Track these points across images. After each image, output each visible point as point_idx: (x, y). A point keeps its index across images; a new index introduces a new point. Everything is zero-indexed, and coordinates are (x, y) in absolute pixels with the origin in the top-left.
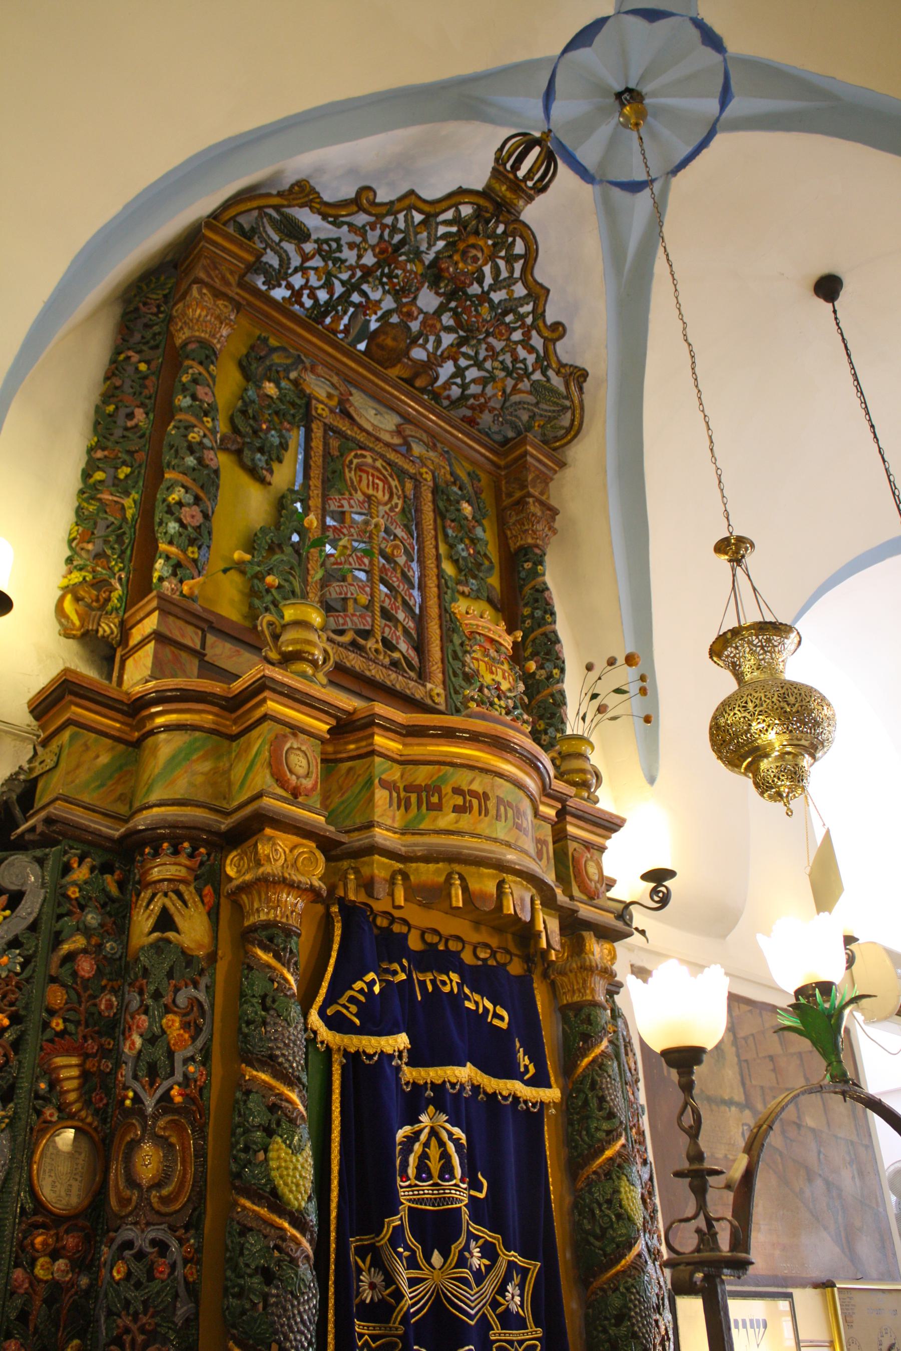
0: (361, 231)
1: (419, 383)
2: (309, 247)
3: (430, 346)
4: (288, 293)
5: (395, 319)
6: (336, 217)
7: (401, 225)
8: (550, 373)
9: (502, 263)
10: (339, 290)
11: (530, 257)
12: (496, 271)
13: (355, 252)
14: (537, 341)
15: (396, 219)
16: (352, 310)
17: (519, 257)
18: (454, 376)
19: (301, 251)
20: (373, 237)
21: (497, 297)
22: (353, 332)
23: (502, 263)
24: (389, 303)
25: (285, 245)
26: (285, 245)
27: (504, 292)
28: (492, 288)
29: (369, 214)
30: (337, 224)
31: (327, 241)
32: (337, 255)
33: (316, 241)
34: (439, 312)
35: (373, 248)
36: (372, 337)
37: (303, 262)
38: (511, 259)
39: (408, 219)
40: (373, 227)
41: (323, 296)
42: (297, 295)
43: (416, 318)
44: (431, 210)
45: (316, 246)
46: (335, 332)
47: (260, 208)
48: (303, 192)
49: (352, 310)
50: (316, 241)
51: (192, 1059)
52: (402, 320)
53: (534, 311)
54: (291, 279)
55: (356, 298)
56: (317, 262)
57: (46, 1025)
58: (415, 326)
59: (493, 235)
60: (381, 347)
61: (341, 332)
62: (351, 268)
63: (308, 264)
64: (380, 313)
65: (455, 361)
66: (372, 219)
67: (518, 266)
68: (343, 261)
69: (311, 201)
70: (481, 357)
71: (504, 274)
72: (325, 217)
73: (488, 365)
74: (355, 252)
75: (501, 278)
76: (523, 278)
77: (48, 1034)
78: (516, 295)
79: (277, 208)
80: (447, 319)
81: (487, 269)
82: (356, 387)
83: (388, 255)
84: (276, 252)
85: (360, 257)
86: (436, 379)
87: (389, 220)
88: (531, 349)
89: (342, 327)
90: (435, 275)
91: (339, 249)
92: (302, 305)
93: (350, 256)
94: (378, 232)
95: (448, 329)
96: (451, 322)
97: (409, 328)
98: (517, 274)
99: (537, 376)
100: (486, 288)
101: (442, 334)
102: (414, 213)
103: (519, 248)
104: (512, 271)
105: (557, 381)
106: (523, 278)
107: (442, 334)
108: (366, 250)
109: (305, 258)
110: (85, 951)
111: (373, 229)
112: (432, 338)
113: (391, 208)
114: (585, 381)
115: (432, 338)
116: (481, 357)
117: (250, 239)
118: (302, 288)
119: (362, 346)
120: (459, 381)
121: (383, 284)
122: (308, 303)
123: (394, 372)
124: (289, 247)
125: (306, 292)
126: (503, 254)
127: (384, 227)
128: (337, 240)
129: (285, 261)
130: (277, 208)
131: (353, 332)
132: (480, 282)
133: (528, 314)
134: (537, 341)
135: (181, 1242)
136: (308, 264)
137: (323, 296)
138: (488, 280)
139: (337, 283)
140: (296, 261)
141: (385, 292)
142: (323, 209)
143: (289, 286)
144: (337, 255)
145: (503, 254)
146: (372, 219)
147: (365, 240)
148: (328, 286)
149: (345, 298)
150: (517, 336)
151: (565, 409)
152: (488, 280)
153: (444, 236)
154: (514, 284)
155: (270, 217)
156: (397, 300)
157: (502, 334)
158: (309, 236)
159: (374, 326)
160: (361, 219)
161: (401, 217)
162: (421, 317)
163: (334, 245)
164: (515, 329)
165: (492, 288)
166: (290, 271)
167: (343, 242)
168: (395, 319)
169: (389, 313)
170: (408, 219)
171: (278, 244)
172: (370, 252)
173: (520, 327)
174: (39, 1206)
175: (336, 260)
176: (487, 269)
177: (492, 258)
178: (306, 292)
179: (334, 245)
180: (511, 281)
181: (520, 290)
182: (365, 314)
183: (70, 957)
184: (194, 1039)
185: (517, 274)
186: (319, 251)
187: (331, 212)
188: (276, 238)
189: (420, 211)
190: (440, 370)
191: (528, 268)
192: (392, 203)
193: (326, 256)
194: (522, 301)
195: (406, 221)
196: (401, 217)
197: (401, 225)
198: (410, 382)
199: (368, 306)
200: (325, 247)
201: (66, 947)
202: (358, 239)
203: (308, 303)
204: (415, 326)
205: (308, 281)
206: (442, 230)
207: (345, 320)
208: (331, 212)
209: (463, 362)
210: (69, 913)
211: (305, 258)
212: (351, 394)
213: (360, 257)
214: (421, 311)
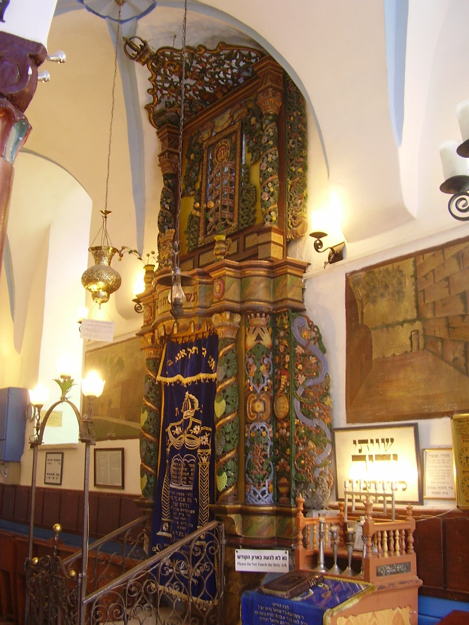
0: (163, 95)
7: (161, 84)
8: (221, 53)
14: (207, 55)
15: (159, 86)
31: (166, 105)
39: (160, 81)
62: (177, 100)
66: (159, 91)
68: (174, 102)
73: (218, 70)
85: (173, 96)
87: (160, 88)
88: (210, 57)
97: (201, 90)
99: (223, 57)
105: (226, 52)
114: (225, 43)
120: (225, 81)
128: (166, 102)
130: (153, 115)
134: (207, 55)
142: (155, 104)
146: (159, 91)
147: (167, 94)
150: (205, 60)
151: (239, 51)
158: (164, 110)
160: (159, 95)
161: (158, 84)
164: (201, 60)
167: (167, 100)
191: (177, 51)
196: (158, 84)
197: (161, 84)
202: (166, 97)
206: (162, 72)
213: (173, 96)
214: (194, 85)
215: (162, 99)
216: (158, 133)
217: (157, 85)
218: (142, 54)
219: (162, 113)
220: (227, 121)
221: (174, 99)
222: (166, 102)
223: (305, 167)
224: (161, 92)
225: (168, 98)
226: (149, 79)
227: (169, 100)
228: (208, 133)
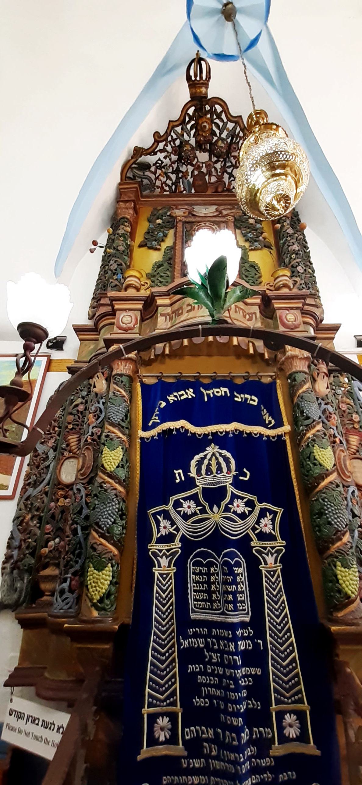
1: (220, 190)
2: (153, 169)
3: (214, 173)
4: (159, 190)
5: (196, 173)
6: (153, 151)
7: (175, 137)
9: (217, 121)
10: (173, 177)
11: (225, 109)
12: (217, 125)
13: (168, 159)
15: (172, 136)
16: (181, 180)
17: (221, 112)
18: (229, 178)
19: (152, 172)
20: (169, 148)
21: (224, 136)
22: (187, 188)
23: (217, 121)
24: (190, 168)
25: (146, 173)
26: (146, 173)
27: (225, 131)
28: (220, 134)
29: (162, 141)
30: (155, 154)
31: (156, 162)
32: (163, 165)
33: (153, 165)
34: (210, 159)
35: (172, 153)
36: (194, 185)
37: (155, 175)
38: (219, 116)
39: (176, 133)
40: (166, 145)
41: (169, 182)
42: (162, 188)
43: (202, 166)
44: (182, 122)
45: (154, 167)
46: (182, 192)
47: (130, 167)
48: (138, 152)
49: (181, 180)
50: (153, 165)
51: (95, 427)
52: (199, 172)
53: (241, 130)
54: (157, 184)
55: (180, 175)
56: (159, 172)
57: (67, 427)
58: (204, 170)
59: (207, 112)
60: (200, 186)
61: (184, 191)
62: (170, 166)
63: (157, 176)
64: (190, 174)
65: (226, 171)
66: (164, 143)
67: (223, 116)
69: (142, 152)
70: (234, 163)
71: (221, 124)
72: (150, 154)
74: (168, 159)
75: (221, 126)
76: (229, 120)
77: (67, 430)
78: (230, 129)
79: (134, 163)
80: (214, 159)
81: (214, 128)
82: (193, 205)
83: (178, 150)
84: (145, 178)
86: (225, 184)
87: (169, 139)
89: (182, 189)
90: (200, 146)
91: (162, 162)
92: (166, 191)
93: (167, 161)
94: (169, 145)
95: (216, 162)
96: (216, 159)
97: (203, 172)
98: (225, 120)
100: (218, 135)
101: (215, 165)
102: (176, 128)
103: (219, 108)
104: (222, 120)
106: (229, 120)
107: (215, 165)
108: (170, 155)
109: (155, 173)
110: (82, 403)
111: (167, 146)
112: (213, 170)
113: (168, 133)
115: (213, 170)
116: (234, 163)
117: (135, 180)
118: (162, 184)
119: (193, 191)
121: (184, 164)
122: (167, 188)
123: (209, 192)
124: (147, 173)
125: (164, 185)
126: (215, 117)
127: (170, 142)
128: (159, 159)
129: (149, 179)
130: (134, 163)
131: (187, 188)
132: (216, 135)
133: (239, 132)
135: (86, 489)
136: (157, 176)
137: (169, 182)
138: (218, 132)
139: (169, 174)
140: (153, 177)
141: (187, 166)
142: (148, 152)
143: (158, 187)
144: (163, 165)
145: (215, 117)
146: (164, 143)
147: (168, 152)
148: (168, 178)
149: (178, 178)
152: (218, 132)
153: (191, 128)
154: (227, 125)
155: (135, 167)
156: (192, 165)
157: (235, 148)
158: (150, 164)
159: (191, 180)
160: (161, 146)
161: (172, 134)
162: (204, 165)
163: (160, 162)
165: (220, 134)
166: (154, 182)
167: (162, 159)
168: (196, 173)
169: (193, 172)
170: (176, 133)
171: (144, 175)
172: (172, 155)
173: (240, 140)
174: (60, 483)
175: (164, 167)
176: (214, 128)
177: (212, 121)
178: (164, 185)
179: (160, 162)
180: (225, 124)
181: (230, 126)
182: (186, 179)
183: (77, 406)
184: (97, 420)
185: (225, 120)
186: (157, 168)
187: (152, 151)
188: (142, 174)
189: (177, 126)
190: (224, 179)
191: (227, 113)
192: (166, 132)
193: (160, 167)
194: (235, 128)
195: (175, 134)
197: (175, 137)
198: (216, 191)
199: (185, 174)
200: (158, 165)
201: (74, 403)
202: (165, 154)
203: (167, 188)
204: (204, 170)
205: (161, 181)
206: (189, 126)
207: (182, 186)
208: (152, 151)
209: (229, 170)
210: (77, 393)
211: (155, 173)
212: (194, 208)
213: (170, 159)
214: (203, 163)
215: (158, 153)
216: (120, 184)
217: (170, 134)
218: (197, 85)
219: (146, 167)
220: (213, 213)
221: (169, 163)
222: (159, 159)
223: (313, 271)
224: (166, 145)
225: (165, 158)
226: (170, 121)
227: (164, 160)
228: (184, 213)
